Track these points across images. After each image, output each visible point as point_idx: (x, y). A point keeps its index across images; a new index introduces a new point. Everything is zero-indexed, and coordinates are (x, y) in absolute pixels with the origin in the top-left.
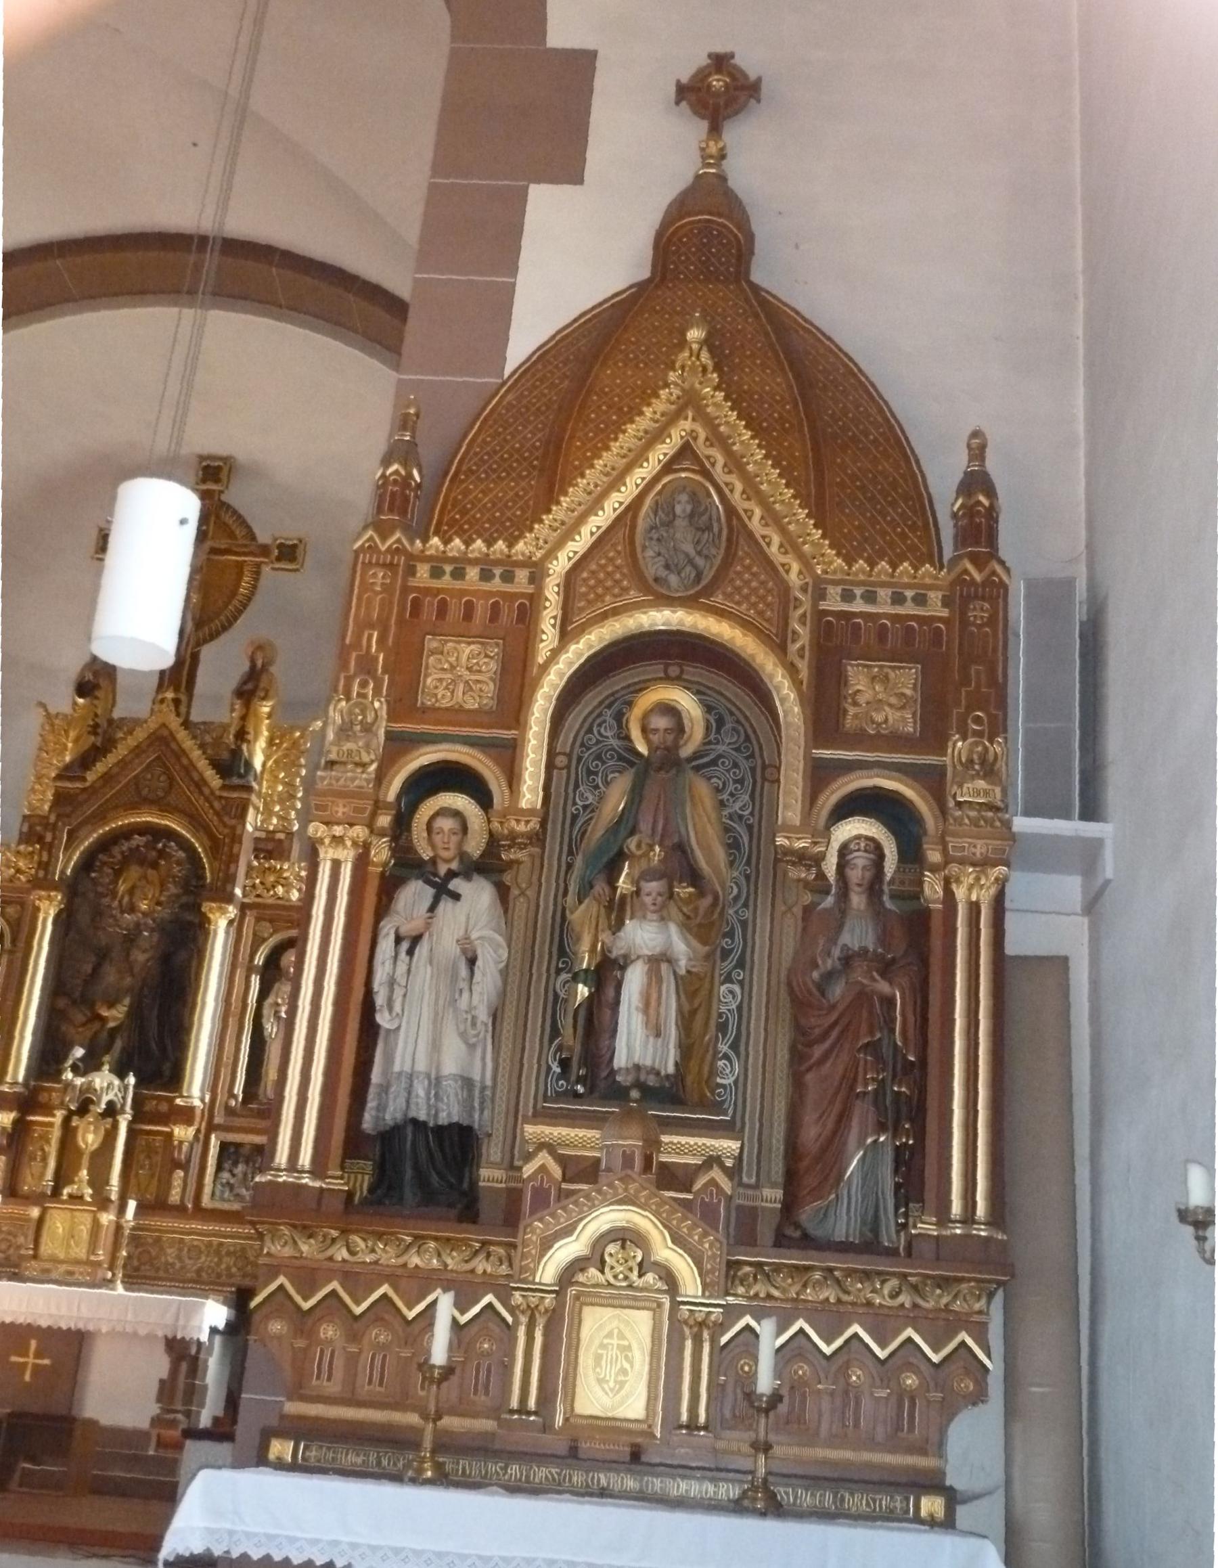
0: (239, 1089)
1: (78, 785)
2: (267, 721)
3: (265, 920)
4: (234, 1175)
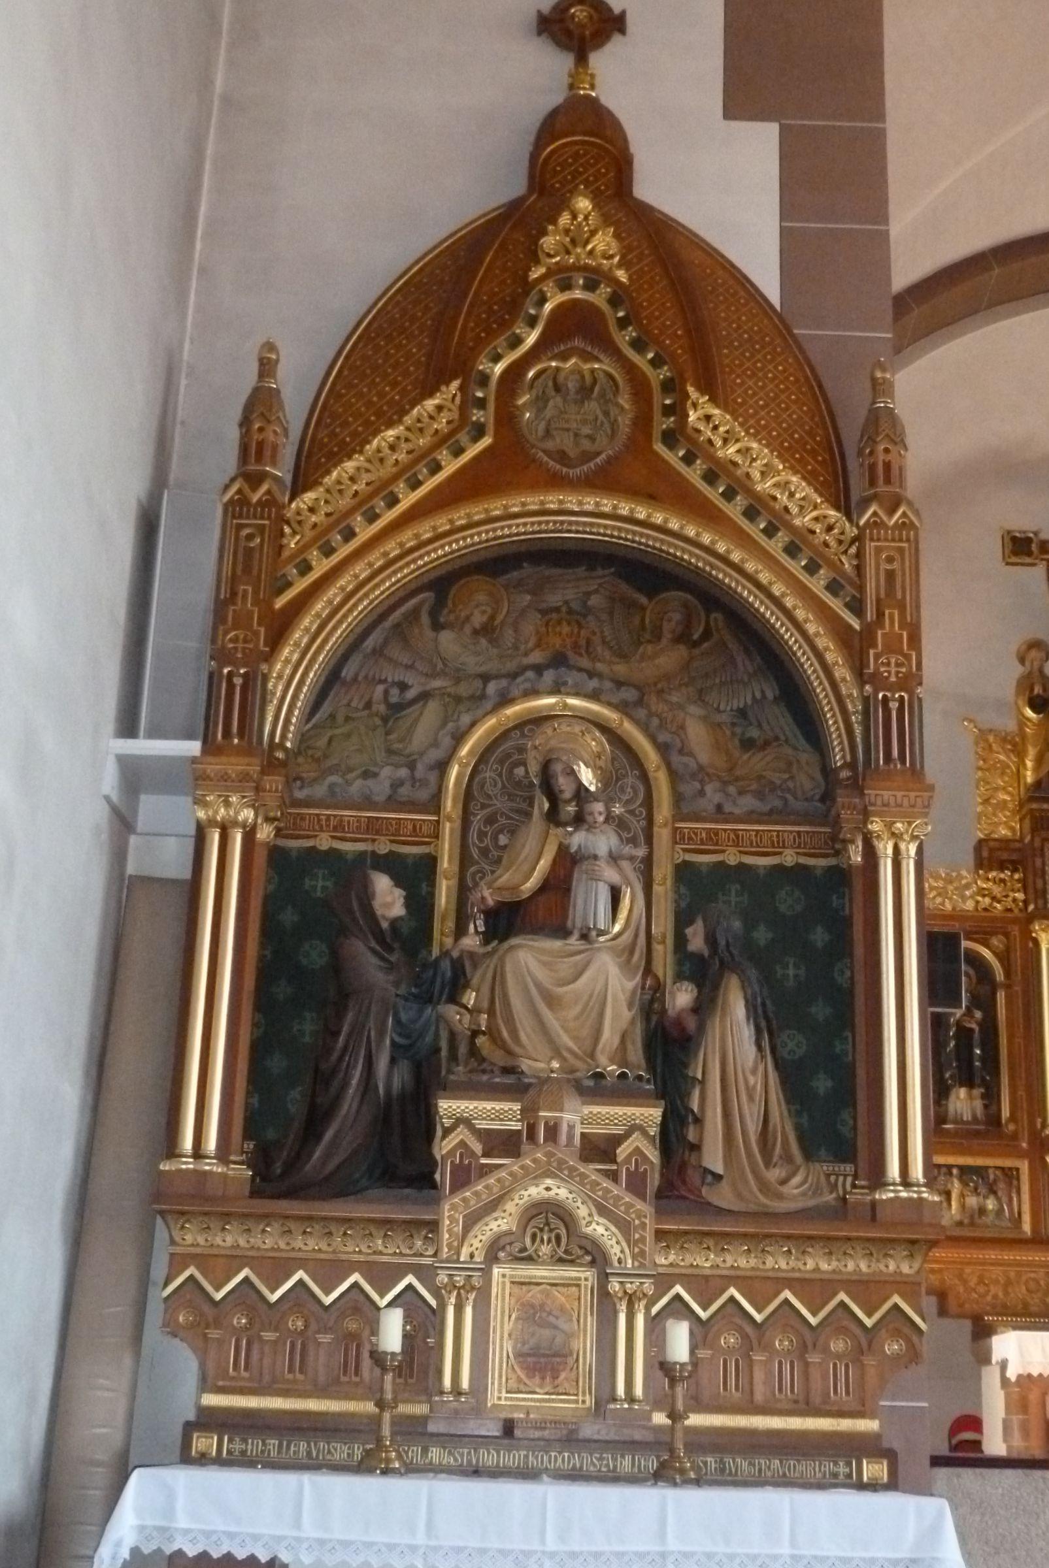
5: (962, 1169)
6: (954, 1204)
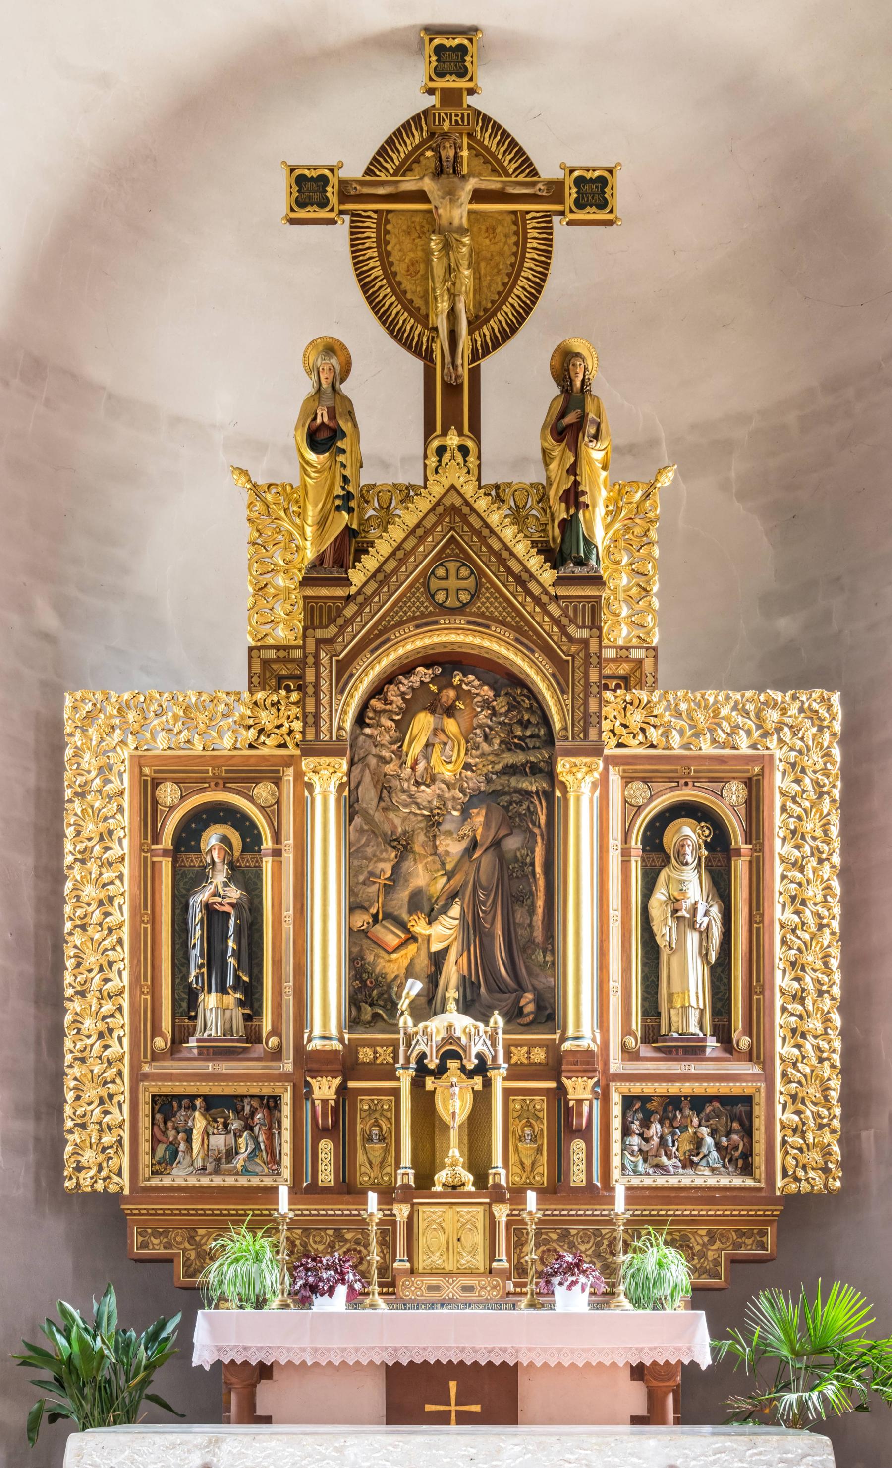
0: (636, 1024)
1: (340, 592)
2: (604, 474)
3: (637, 779)
4: (647, 1140)
5: (206, 1098)
6: (196, 1145)
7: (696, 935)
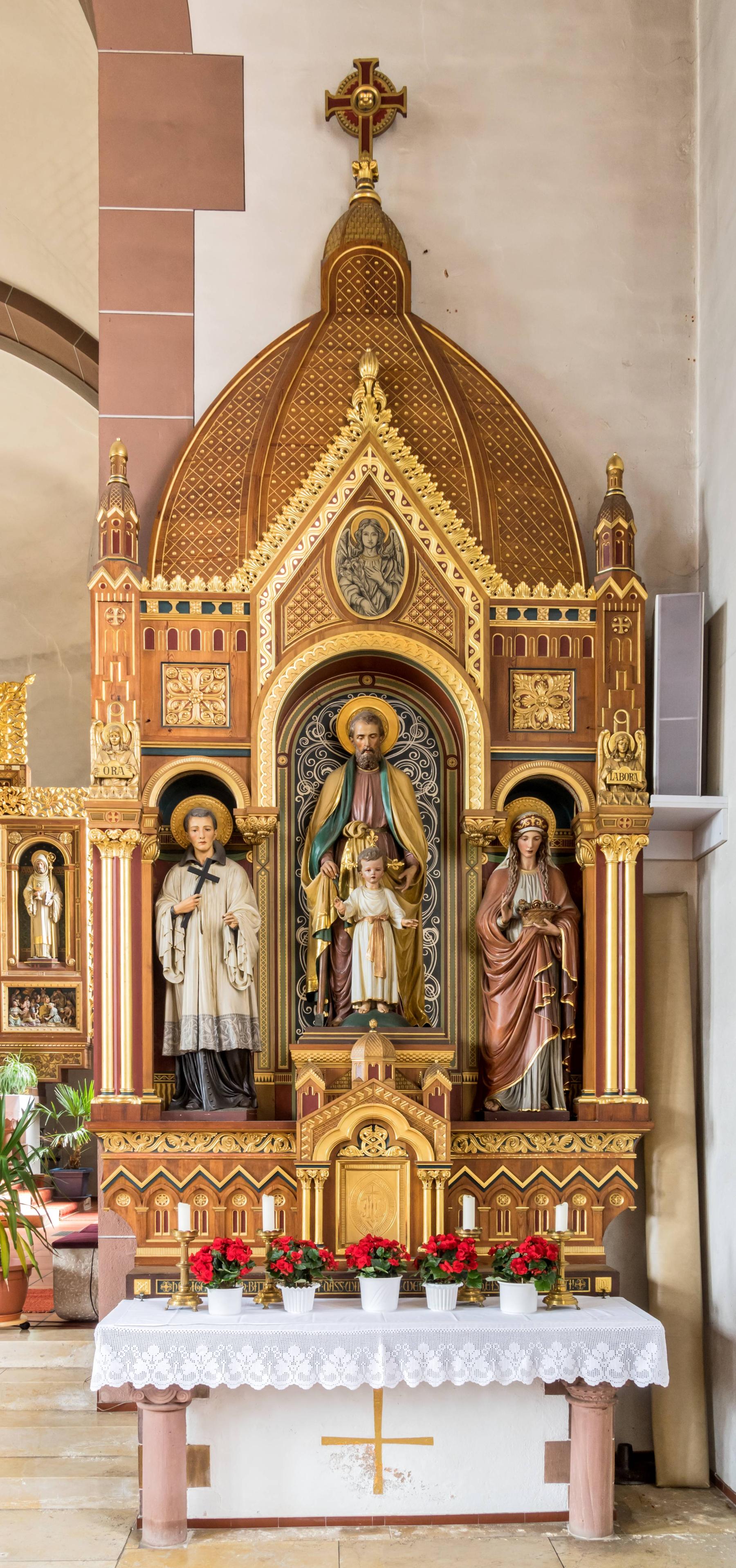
0: (16, 951)
4: (22, 1009)
7: (47, 909)
